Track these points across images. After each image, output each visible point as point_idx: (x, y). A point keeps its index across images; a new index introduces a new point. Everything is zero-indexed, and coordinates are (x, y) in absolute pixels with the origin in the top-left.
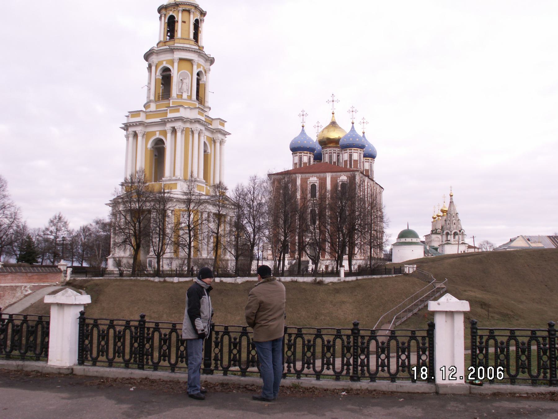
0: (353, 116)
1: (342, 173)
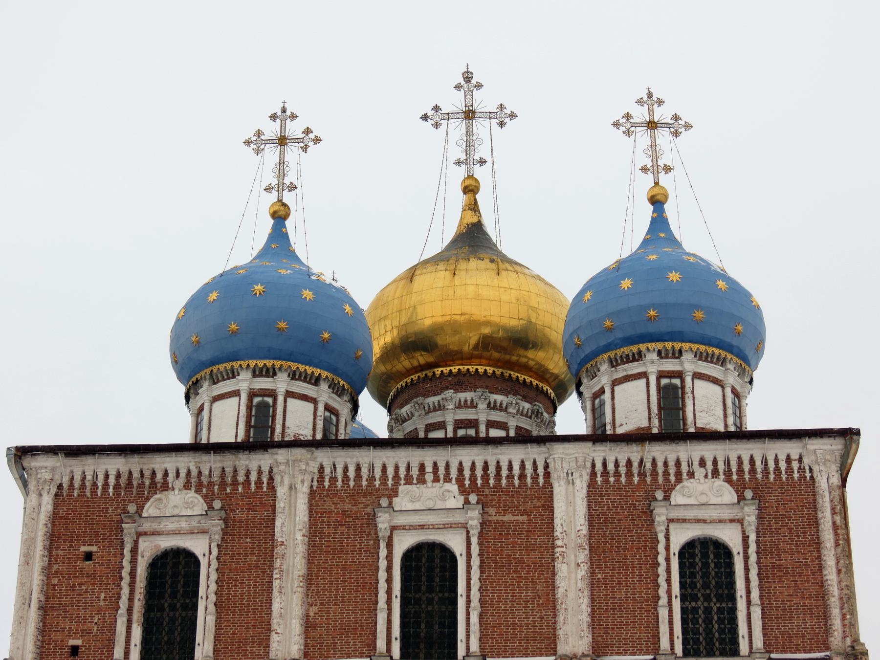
0: (655, 157)
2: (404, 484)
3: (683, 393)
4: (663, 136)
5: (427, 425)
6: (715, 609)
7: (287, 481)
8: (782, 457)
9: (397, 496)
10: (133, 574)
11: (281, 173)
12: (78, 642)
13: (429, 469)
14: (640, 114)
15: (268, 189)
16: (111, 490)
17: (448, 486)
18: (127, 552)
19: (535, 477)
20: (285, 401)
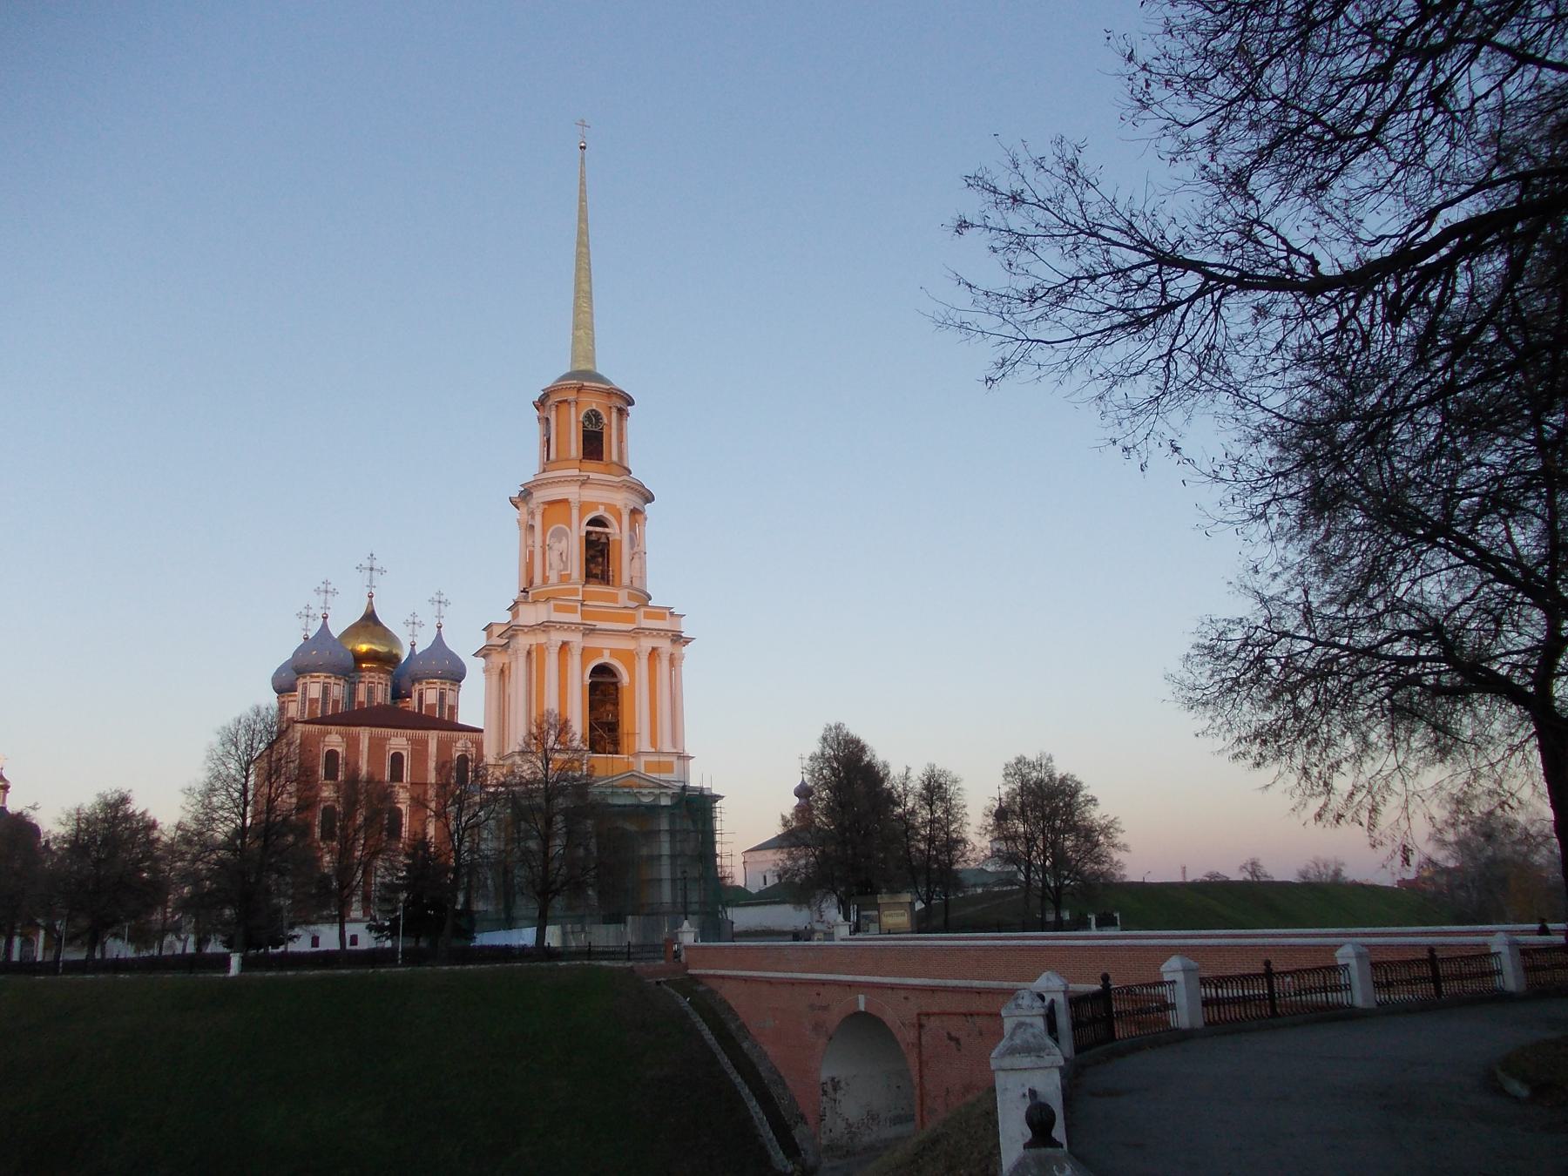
4: (442, 606)
14: (437, 598)
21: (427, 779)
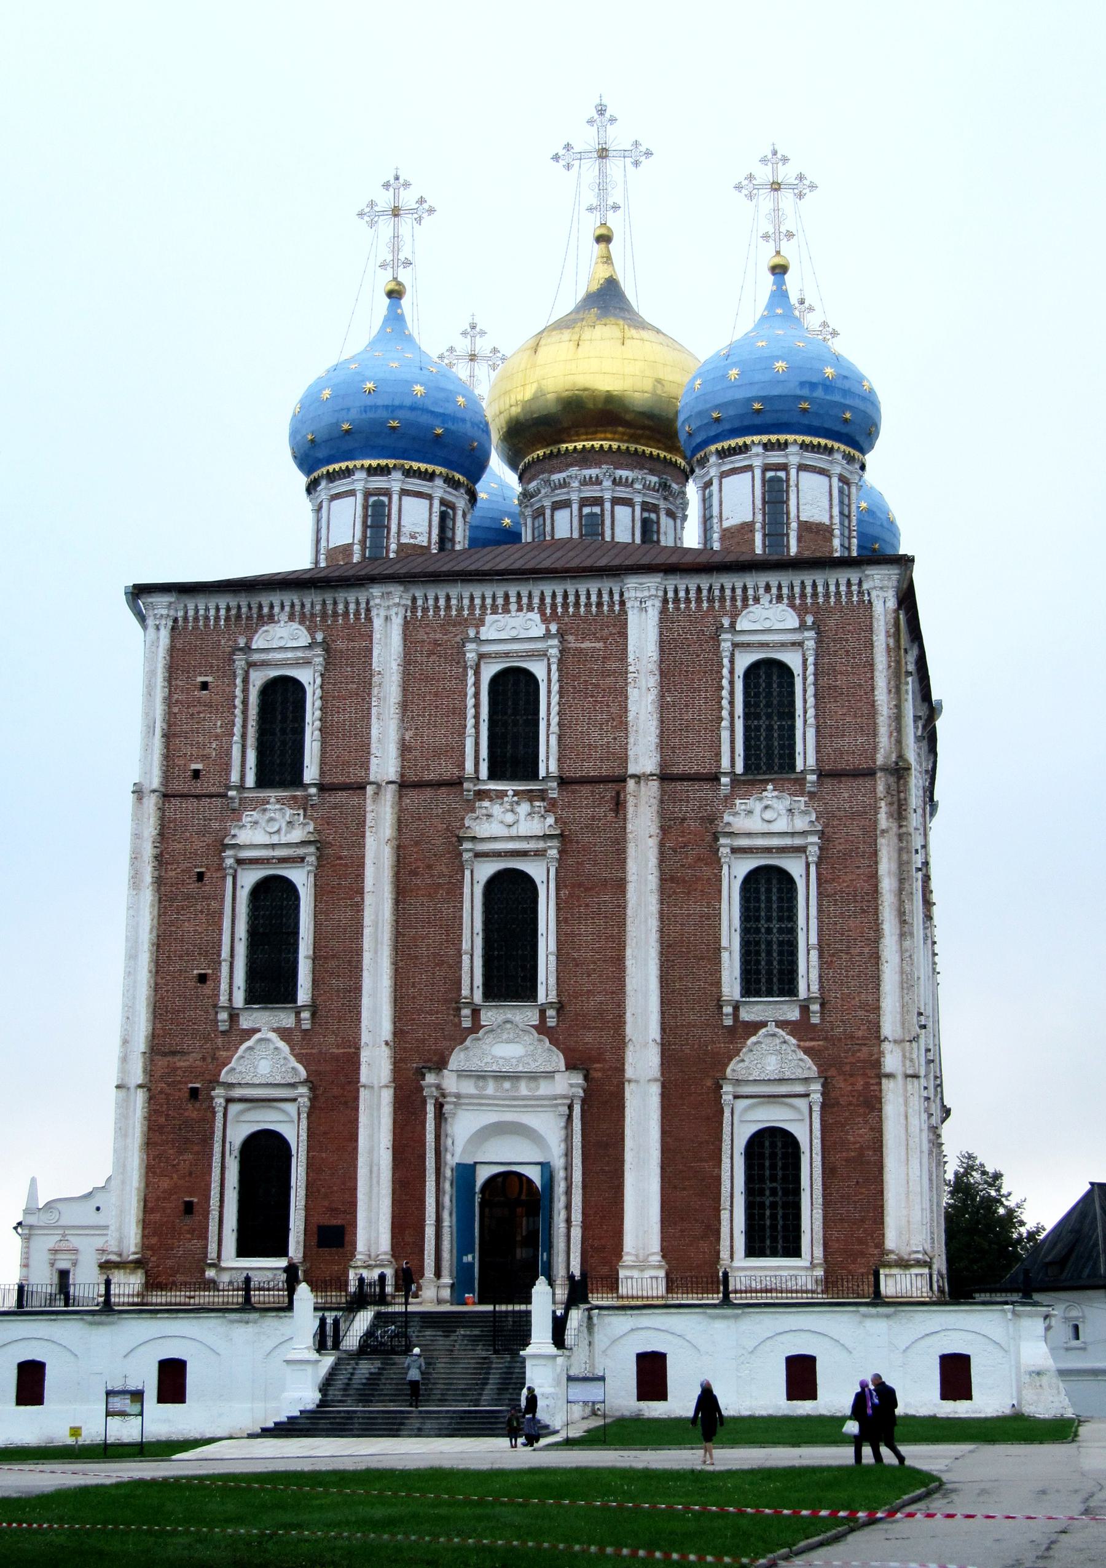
1: (754, 581)
2: (491, 614)
3: (788, 486)
5: (553, 503)
6: (776, 727)
7: (383, 613)
8: (843, 582)
9: (483, 625)
10: (245, 702)
11: (396, 248)
12: (199, 766)
13: (513, 599)
14: (764, 174)
15: (383, 266)
16: (222, 623)
17: (530, 615)
18: (239, 681)
19: (611, 604)
20: (400, 500)
21: (624, 760)
